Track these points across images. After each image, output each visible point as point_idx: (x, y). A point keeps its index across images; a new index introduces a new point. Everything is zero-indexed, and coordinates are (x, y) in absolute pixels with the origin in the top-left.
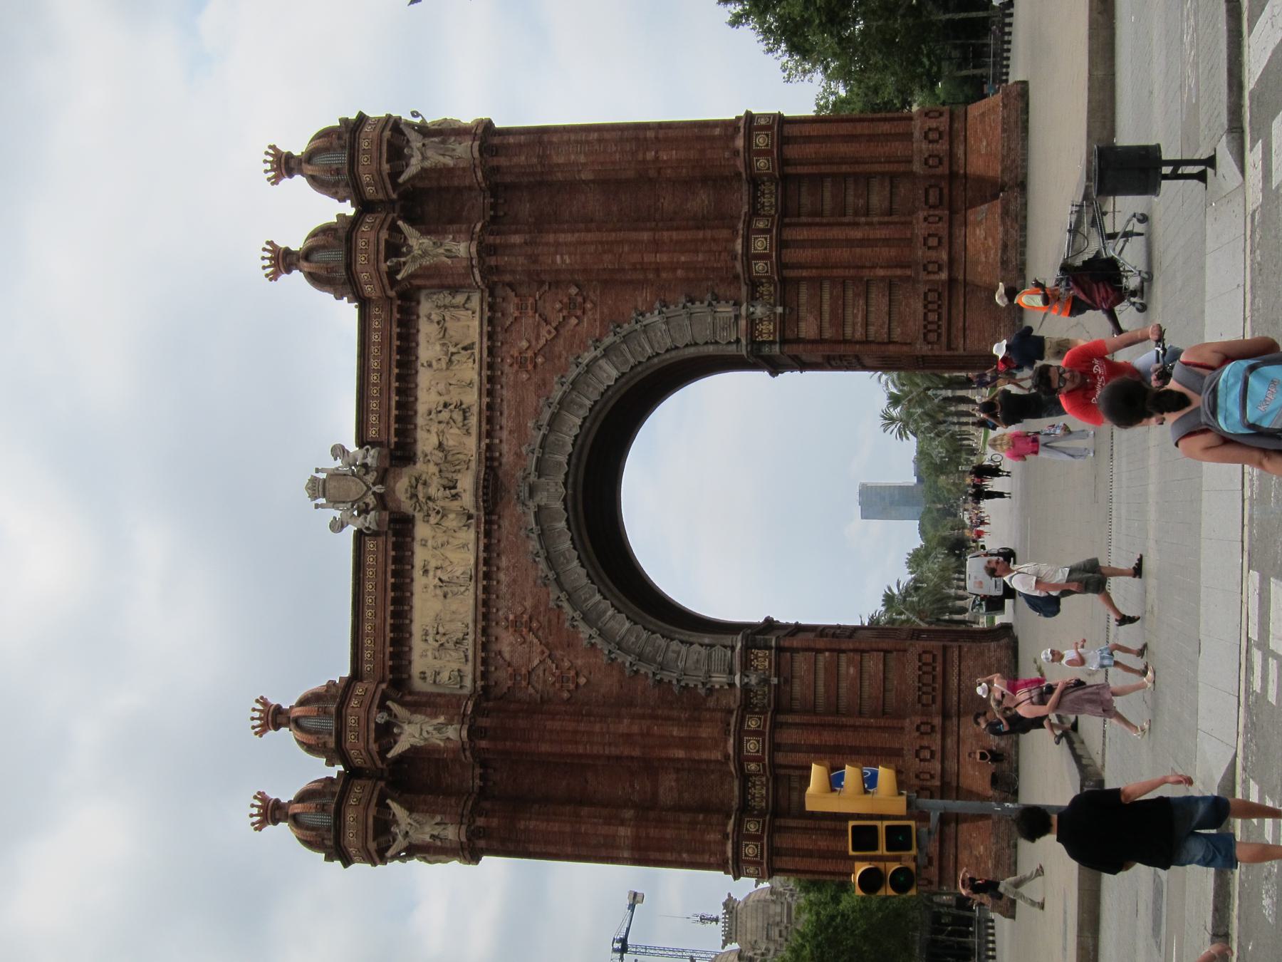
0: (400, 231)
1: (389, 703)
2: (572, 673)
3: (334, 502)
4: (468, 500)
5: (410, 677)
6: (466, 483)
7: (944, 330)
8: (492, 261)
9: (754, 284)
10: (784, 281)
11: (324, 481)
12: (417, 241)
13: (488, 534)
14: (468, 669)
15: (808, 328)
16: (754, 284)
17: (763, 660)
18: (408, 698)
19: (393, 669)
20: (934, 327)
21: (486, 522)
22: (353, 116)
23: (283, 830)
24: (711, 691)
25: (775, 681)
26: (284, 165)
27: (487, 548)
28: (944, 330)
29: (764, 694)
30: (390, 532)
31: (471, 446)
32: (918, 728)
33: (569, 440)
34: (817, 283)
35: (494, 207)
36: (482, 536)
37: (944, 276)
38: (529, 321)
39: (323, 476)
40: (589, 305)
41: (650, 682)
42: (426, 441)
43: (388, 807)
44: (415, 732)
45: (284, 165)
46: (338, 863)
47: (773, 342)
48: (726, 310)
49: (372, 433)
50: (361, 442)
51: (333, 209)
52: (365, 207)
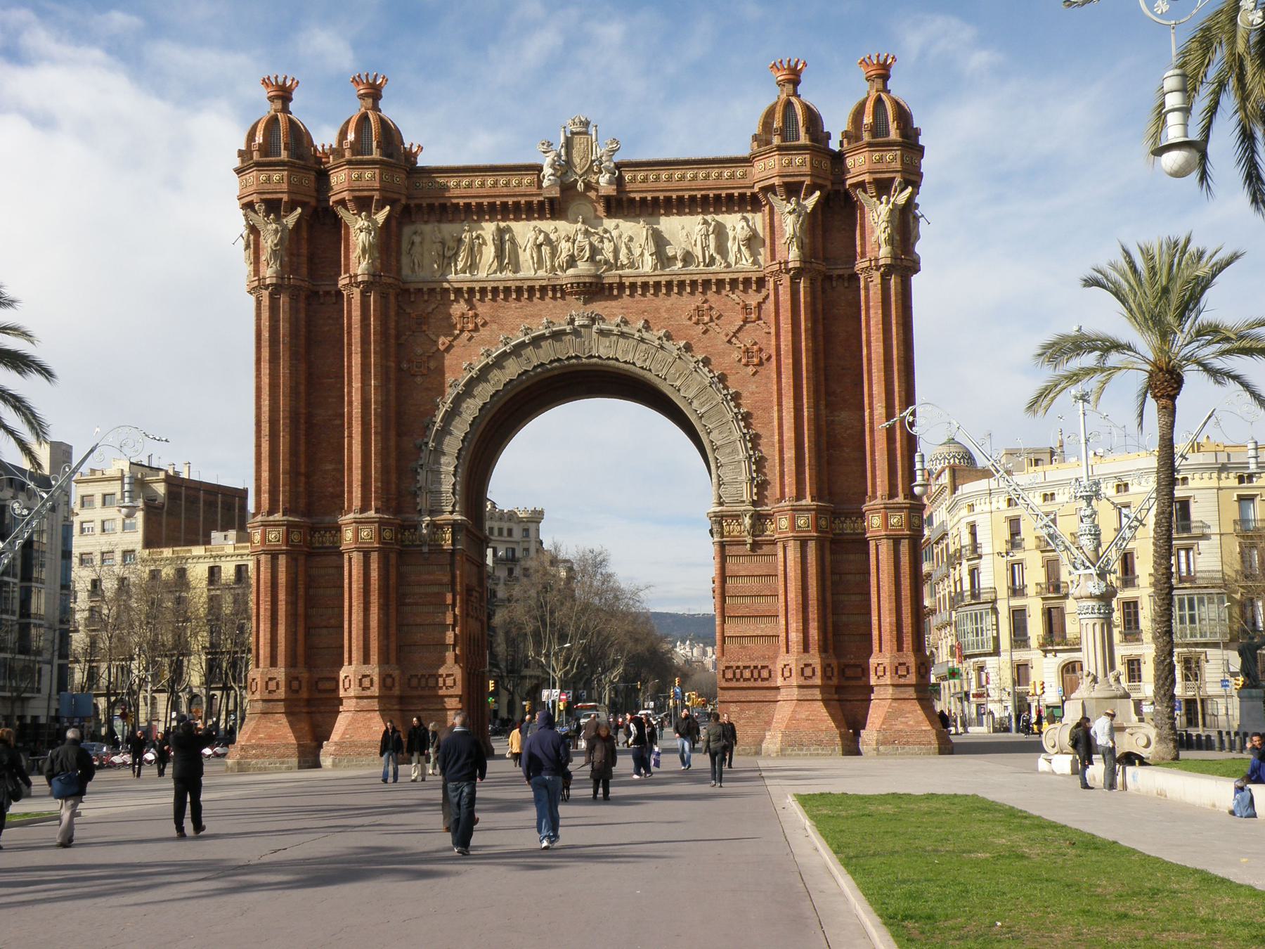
0: (812, 193)
1: (388, 208)
2: (425, 371)
3: (569, 144)
5: (413, 222)
7: (734, 684)
8: (786, 280)
10: (774, 543)
11: (586, 133)
13: (543, 289)
14: (423, 274)
16: (769, 516)
18: (394, 223)
19: (419, 206)
20: (738, 676)
21: (554, 287)
22: (922, 141)
24: (415, 495)
25: (425, 549)
27: (531, 290)
28: (734, 684)
29: (413, 541)
30: (541, 199)
32: (390, 676)
33: (629, 358)
35: (840, 276)
36: (544, 283)
37: (780, 682)
39: (592, 131)
40: (751, 369)
41: (419, 442)
43: (293, 209)
46: (237, 163)
47: (722, 536)
48: (746, 493)
49: (627, 177)
50: (619, 166)
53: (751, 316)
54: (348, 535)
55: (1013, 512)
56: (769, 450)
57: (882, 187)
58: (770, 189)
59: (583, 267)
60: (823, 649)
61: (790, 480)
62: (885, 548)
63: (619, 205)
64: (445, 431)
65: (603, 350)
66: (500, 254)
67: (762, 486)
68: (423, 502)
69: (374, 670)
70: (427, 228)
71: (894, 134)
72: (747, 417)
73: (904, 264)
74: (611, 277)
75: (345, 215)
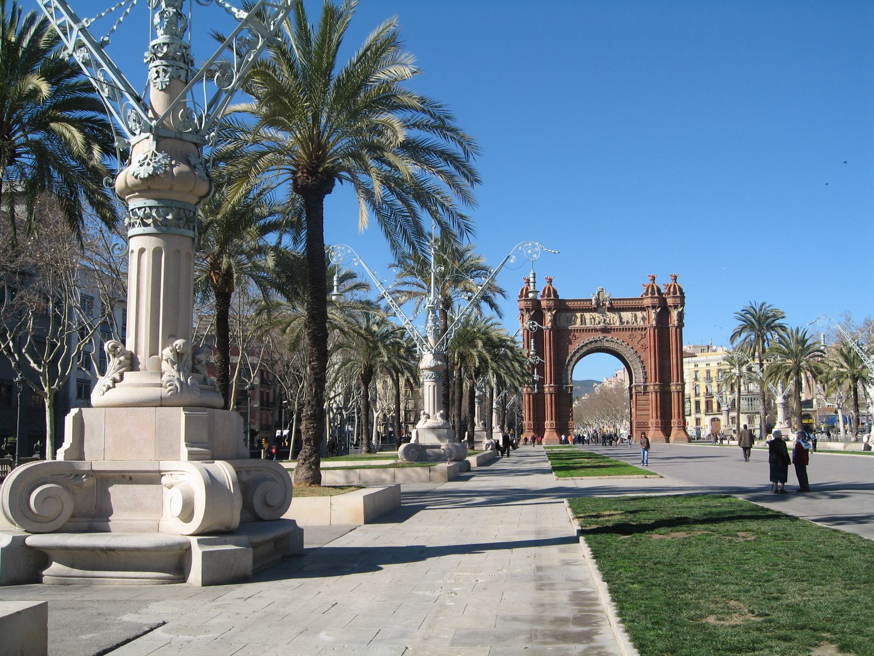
3: (598, 294)
48: (642, 380)
53: (643, 337)
54: (546, 390)
55: (696, 369)
56: (648, 370)
57: (676, 307)
58: (648, 307)
59: (602, 324)
60: (661, 418)
61: (653, 377)
62: (676, 394)
63: (612, 309)
64: (569, 364)
65: (607, 345)
66: (581, 321)
67: (646, 379)
68: (564, 381)
69: (554, 422)
70: (563, 314)
71: (678, 294)
72: (642, 362)
73: (681, 325)
74: (609, 327)
75: (545, 312)
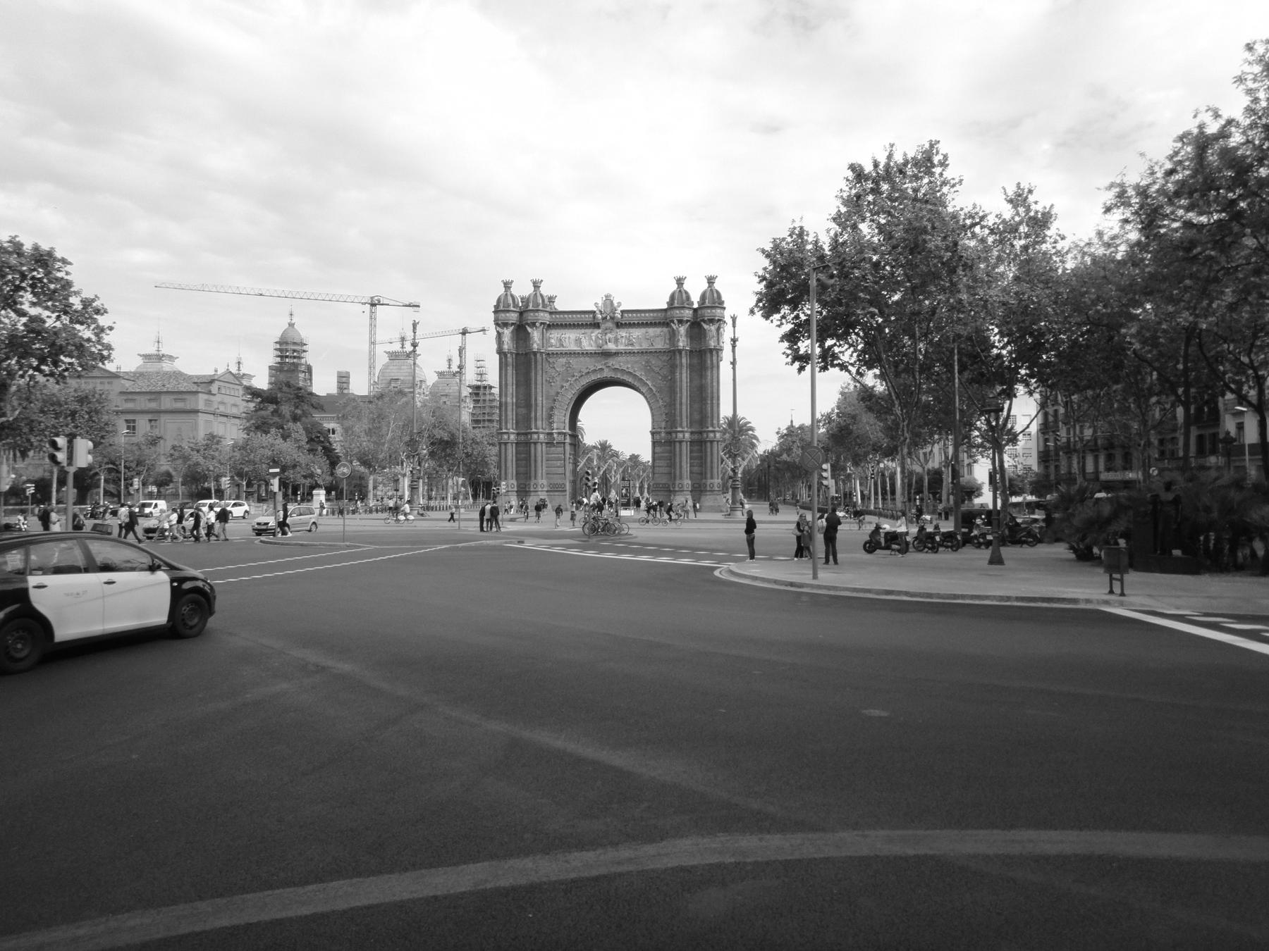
3: (605, 304)
4: (605, 347)
6: (611, 346)
9: (670, 433)
12: (682, 330)
15: (658, 449)
17: (561, 438)
23: (501, 290)
26: (711, 281)
31: (621, 347)
34: (670, 452)
38: (660, 363)
42: (623, 333)
44: (536, 335)
45: (711, 281)
48: (663, 425)
50: (623, 312)
51: (695, 299)
52: (695, 310)
